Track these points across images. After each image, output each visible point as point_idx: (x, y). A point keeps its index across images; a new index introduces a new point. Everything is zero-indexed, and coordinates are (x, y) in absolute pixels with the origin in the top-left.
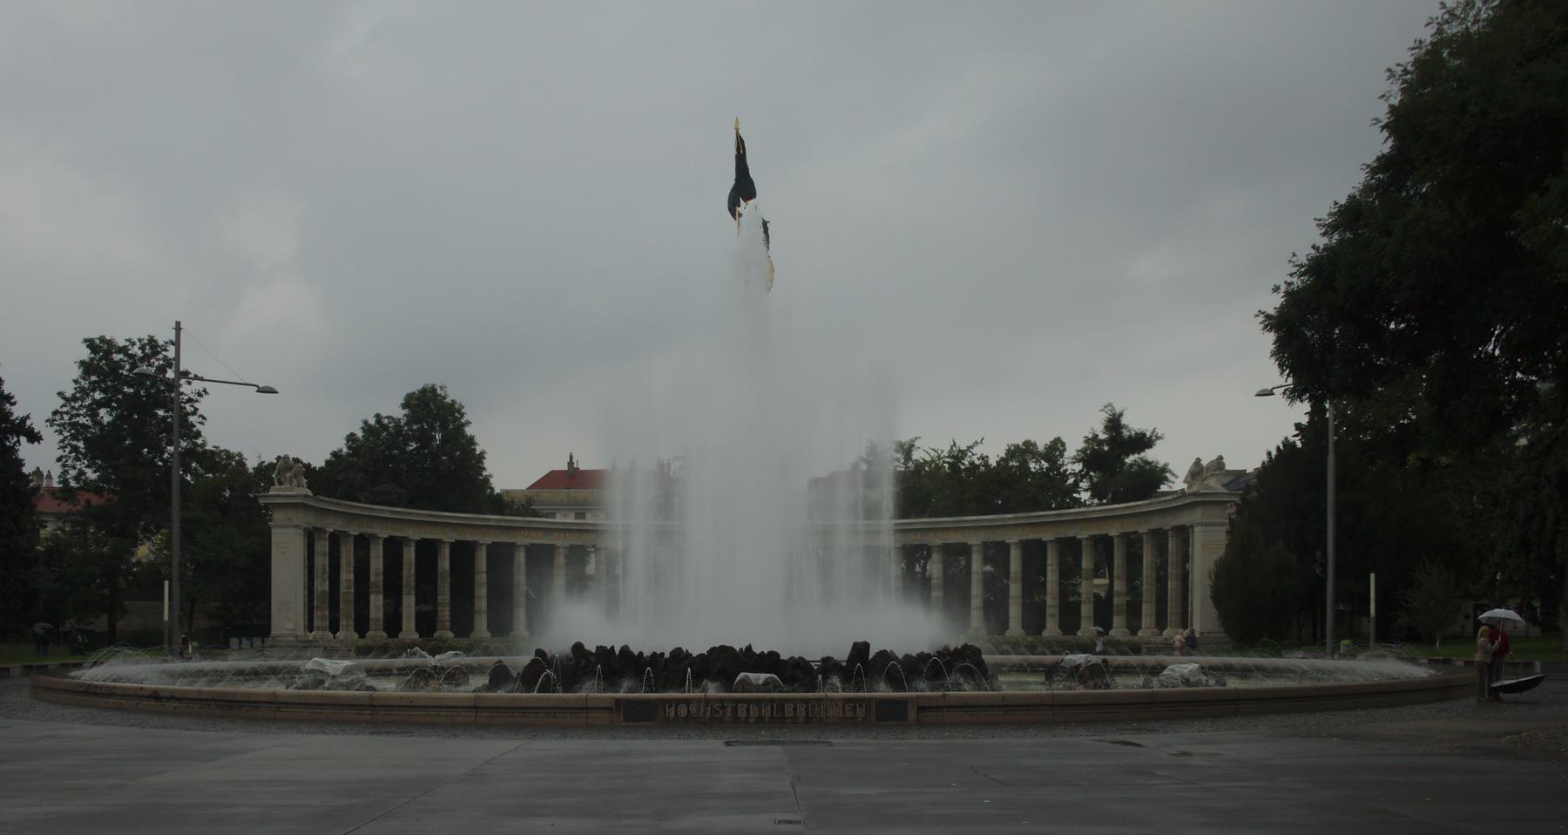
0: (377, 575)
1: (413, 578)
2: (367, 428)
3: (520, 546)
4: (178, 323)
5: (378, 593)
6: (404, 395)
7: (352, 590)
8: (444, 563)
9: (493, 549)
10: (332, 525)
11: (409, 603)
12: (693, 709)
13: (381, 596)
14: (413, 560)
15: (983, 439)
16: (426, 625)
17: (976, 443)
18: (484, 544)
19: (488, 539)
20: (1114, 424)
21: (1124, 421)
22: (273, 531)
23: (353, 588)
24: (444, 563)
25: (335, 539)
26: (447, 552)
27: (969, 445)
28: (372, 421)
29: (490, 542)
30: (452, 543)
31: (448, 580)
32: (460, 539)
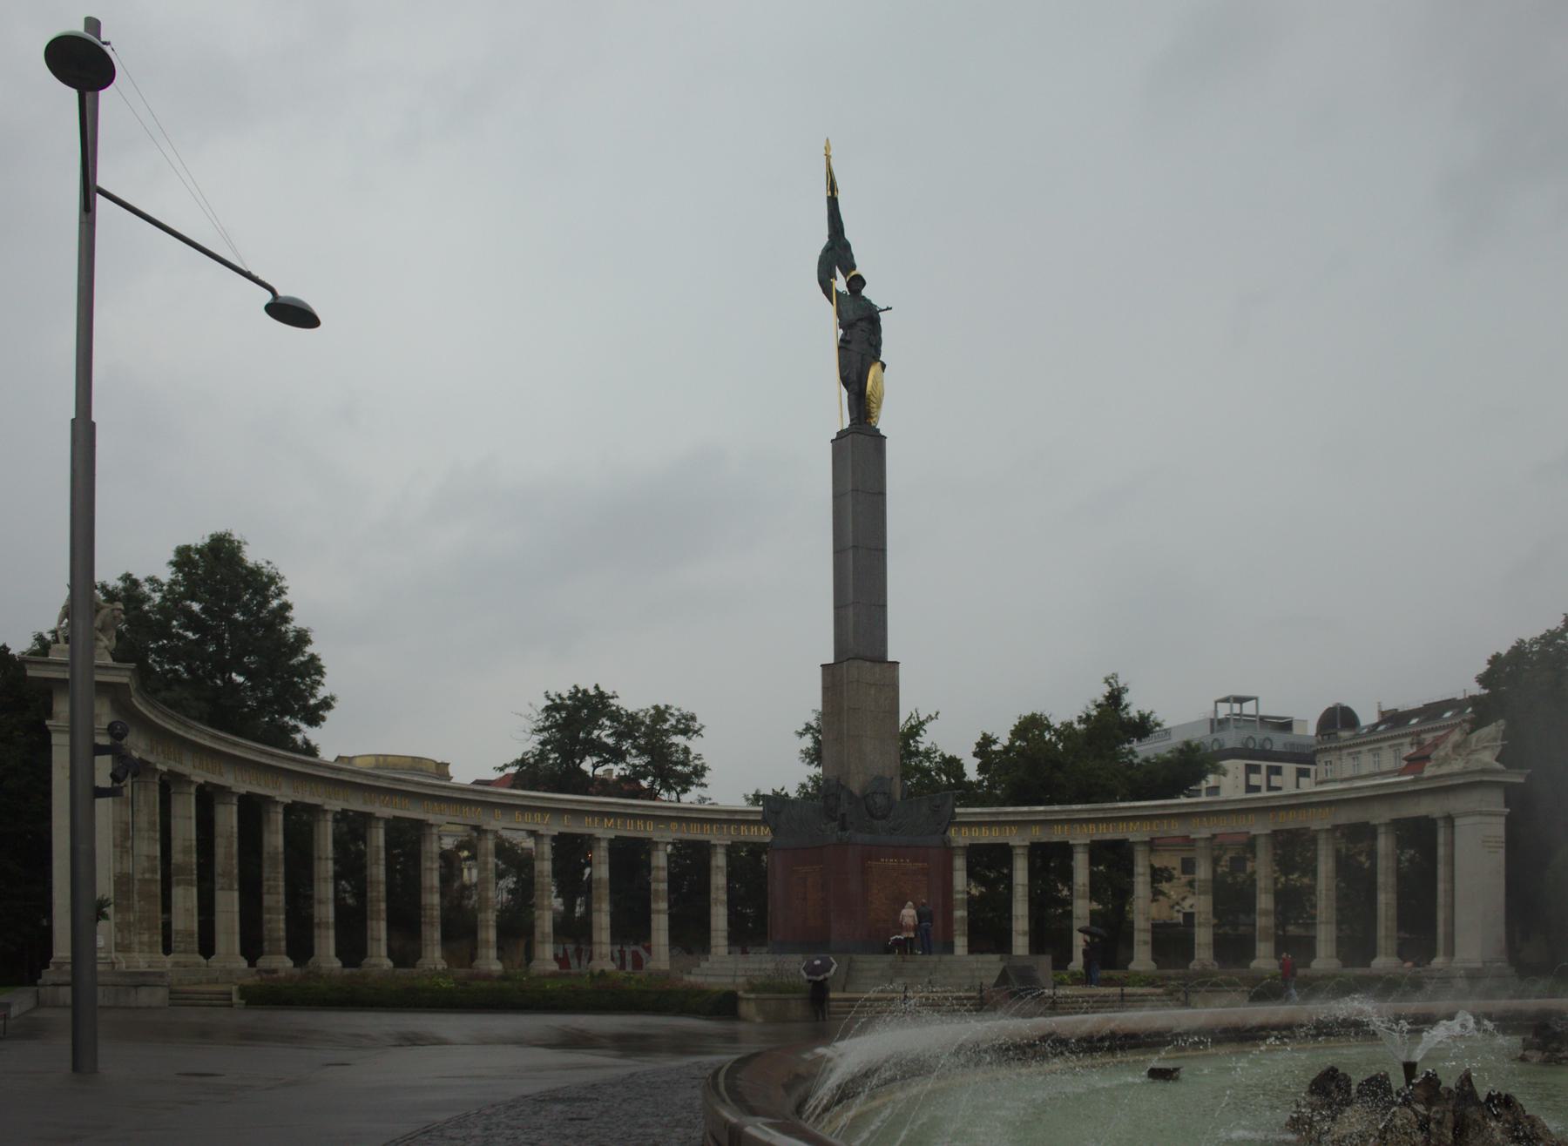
0: (186, 851)
1: (235, 861)
5: (189, 883)
7: (159, 877)
8: (275, 839)
11: (228, 904)
13: (195, 890)
14: (235, 830)
15: (937, 714)
17: (930, 718)
18: (331, 811)
23: (159, 872)
24: (275, 839)
26: (280, 818)
30: (288, 804)
31: (282, 869)
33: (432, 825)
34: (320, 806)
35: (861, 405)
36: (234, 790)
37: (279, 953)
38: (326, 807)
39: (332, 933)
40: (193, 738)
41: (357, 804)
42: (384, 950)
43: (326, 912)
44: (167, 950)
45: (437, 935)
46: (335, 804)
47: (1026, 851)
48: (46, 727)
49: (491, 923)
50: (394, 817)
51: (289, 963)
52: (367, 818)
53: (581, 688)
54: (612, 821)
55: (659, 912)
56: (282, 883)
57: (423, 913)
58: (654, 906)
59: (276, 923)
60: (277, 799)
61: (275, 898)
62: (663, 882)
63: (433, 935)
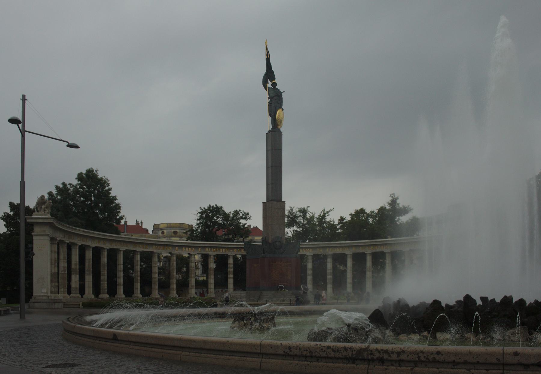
0: (76, 265)
1: (91, 267)
3: (138, 252)
4: (24, 96)
5: (76, 274)
6: (77, 174)
7: (66, 272)
8: (104, 260)
9: (126, 253)
10: (59, 237)
11: (89, 279)
13: (78, 276)
14: (91, 258)
15: (333, 208)
16: (97, 290)
17: (331, 210)
18: (122, 250)
19: (124, 248)
20: (393, 202)
21: (398, 201)
22: (34, 238)
23: (66, 271)
24: (104, 260)
25: (59, 244)
27: (327, 211)
29: (125, 250)
30: (108, 249)
31: (106, 268)
32: (112, 247)
33: (155, 253)
34: (118, 249)
36: (90, 246)
37: (105, 293)
38: (121, 249)
39: (122, 287)
40: (77, 232)
41: (131, 248)
42: (139, 292)
44: (69, 292)
45: (157, 287)
47: (351, 256)
48: (32, 234)
49: (174, 283)
50: (143, 251)
51: (108, 296)
53: (212, 206)
54: (215, 249)
55: (230, 278)
56: (106, 273)
57: (152, 280)
58: (229, 276)
59: (104, 284)
60: (105, 248)
61: (104, 277)
62: (232, 268)
63: (156, 287)
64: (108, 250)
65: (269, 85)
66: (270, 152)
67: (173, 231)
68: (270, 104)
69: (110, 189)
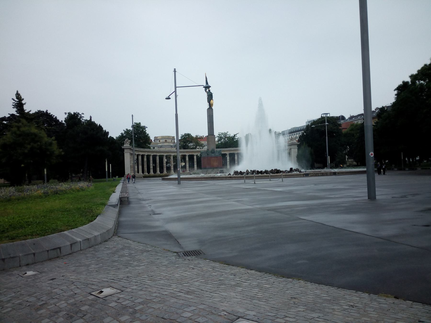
2: (125, 132)
5: (136, 165)
8: (145, 159)
11: (140, 167)
12: (313, 174)
17: (237, 134)
24: (145, 159)
28: (125, 130)
35: (211, 106)
39: (152, 170)
41: (155, 154)
43: (151, 167)
46: (152, 154)
52: (156, 155)
56: (146, 164)
58: (195, 163)
59: (146, 169)
61: (145, 166)
63: (165, 169)
64: (147, 155)
65: (207, 90)
66: (208, 117)
67: (165, 140)
68: (208, 98)
69: (146, 131)
